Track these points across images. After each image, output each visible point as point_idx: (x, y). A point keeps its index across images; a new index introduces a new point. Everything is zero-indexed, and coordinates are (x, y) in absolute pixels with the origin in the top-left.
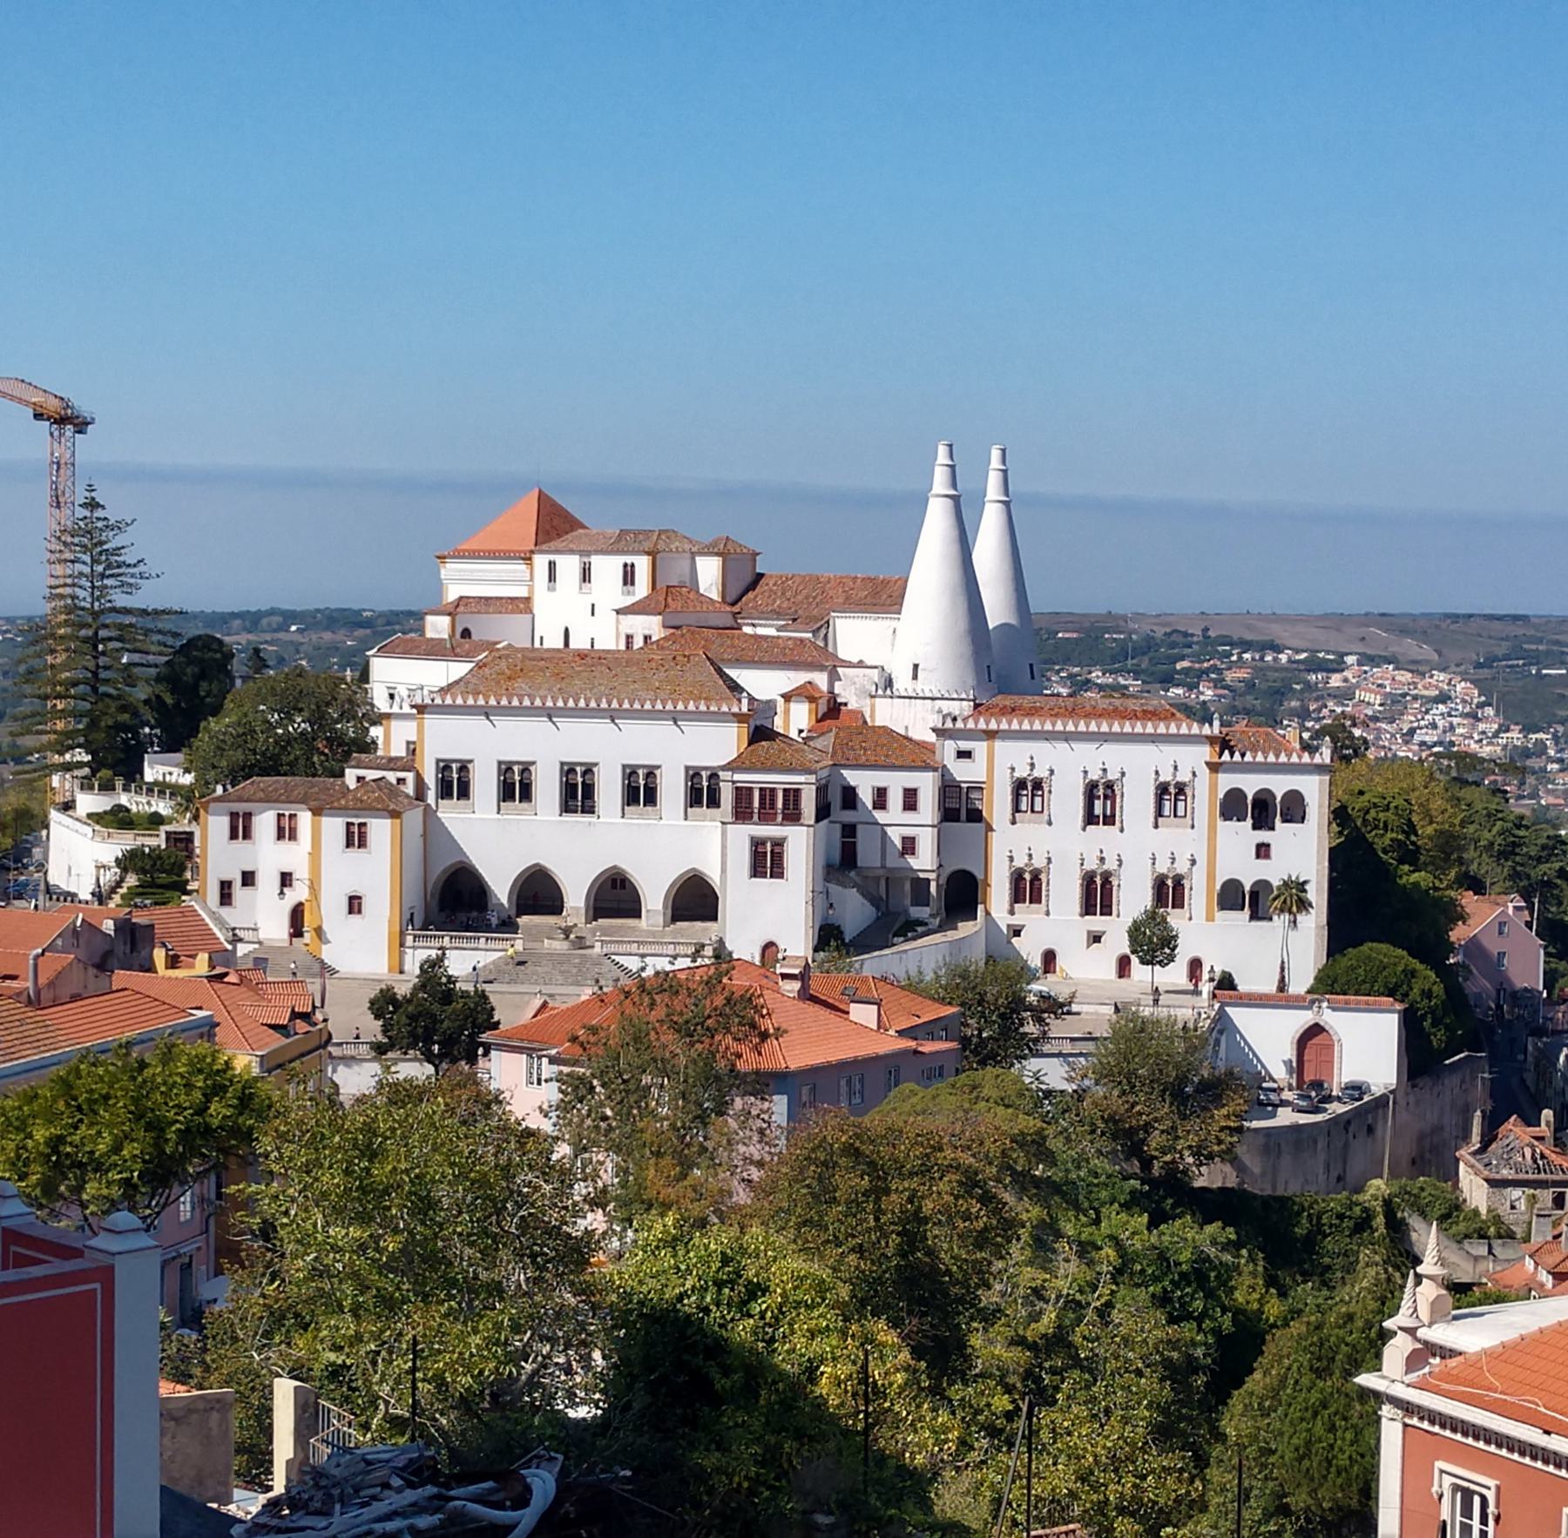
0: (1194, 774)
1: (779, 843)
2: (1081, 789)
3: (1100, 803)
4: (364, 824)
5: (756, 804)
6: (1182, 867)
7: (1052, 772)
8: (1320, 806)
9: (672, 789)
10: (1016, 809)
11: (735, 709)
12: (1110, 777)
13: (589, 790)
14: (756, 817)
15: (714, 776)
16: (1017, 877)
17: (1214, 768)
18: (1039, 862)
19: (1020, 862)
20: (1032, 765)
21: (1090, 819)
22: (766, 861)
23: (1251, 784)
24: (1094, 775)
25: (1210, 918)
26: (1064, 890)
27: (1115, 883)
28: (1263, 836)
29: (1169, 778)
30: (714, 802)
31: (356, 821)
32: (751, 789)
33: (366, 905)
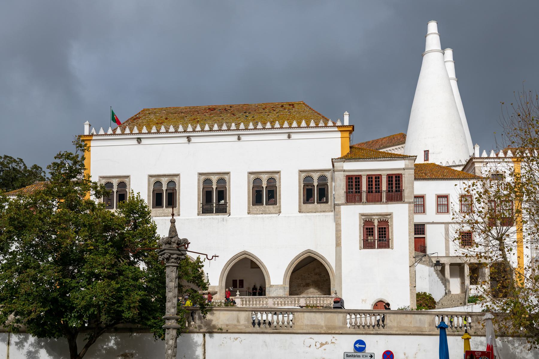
9: (290, 191)
13: (222, 194)
15: (323, 179)
22: (376, 235)
32: (361, 176)
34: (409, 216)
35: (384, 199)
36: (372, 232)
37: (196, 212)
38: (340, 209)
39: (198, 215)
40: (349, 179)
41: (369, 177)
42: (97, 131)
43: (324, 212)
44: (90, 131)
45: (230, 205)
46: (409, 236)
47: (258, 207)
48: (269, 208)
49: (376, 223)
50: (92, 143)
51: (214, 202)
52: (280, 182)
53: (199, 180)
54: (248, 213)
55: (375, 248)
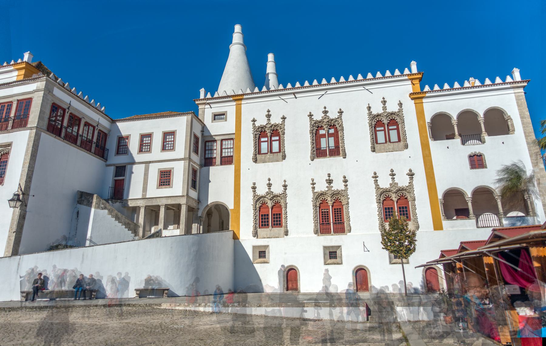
0: (400, 104)
2: (308, 129)
3: (327, 139)
6: (403, 181)
7: (284, 118)
8: (522, 117)
10: (258, 151)
12: (333, 115)
16: (260, 203)
17: (417, 97)
18: (277, 189)
19: (262, 191)
20: (269, 116)
21: (318, 152)
24: (318, 116)
25: (438, 227)
26: (300, 214)
27: (344, 202)
29: (381, 111)
34: (28, 144)
46: (23, 167)
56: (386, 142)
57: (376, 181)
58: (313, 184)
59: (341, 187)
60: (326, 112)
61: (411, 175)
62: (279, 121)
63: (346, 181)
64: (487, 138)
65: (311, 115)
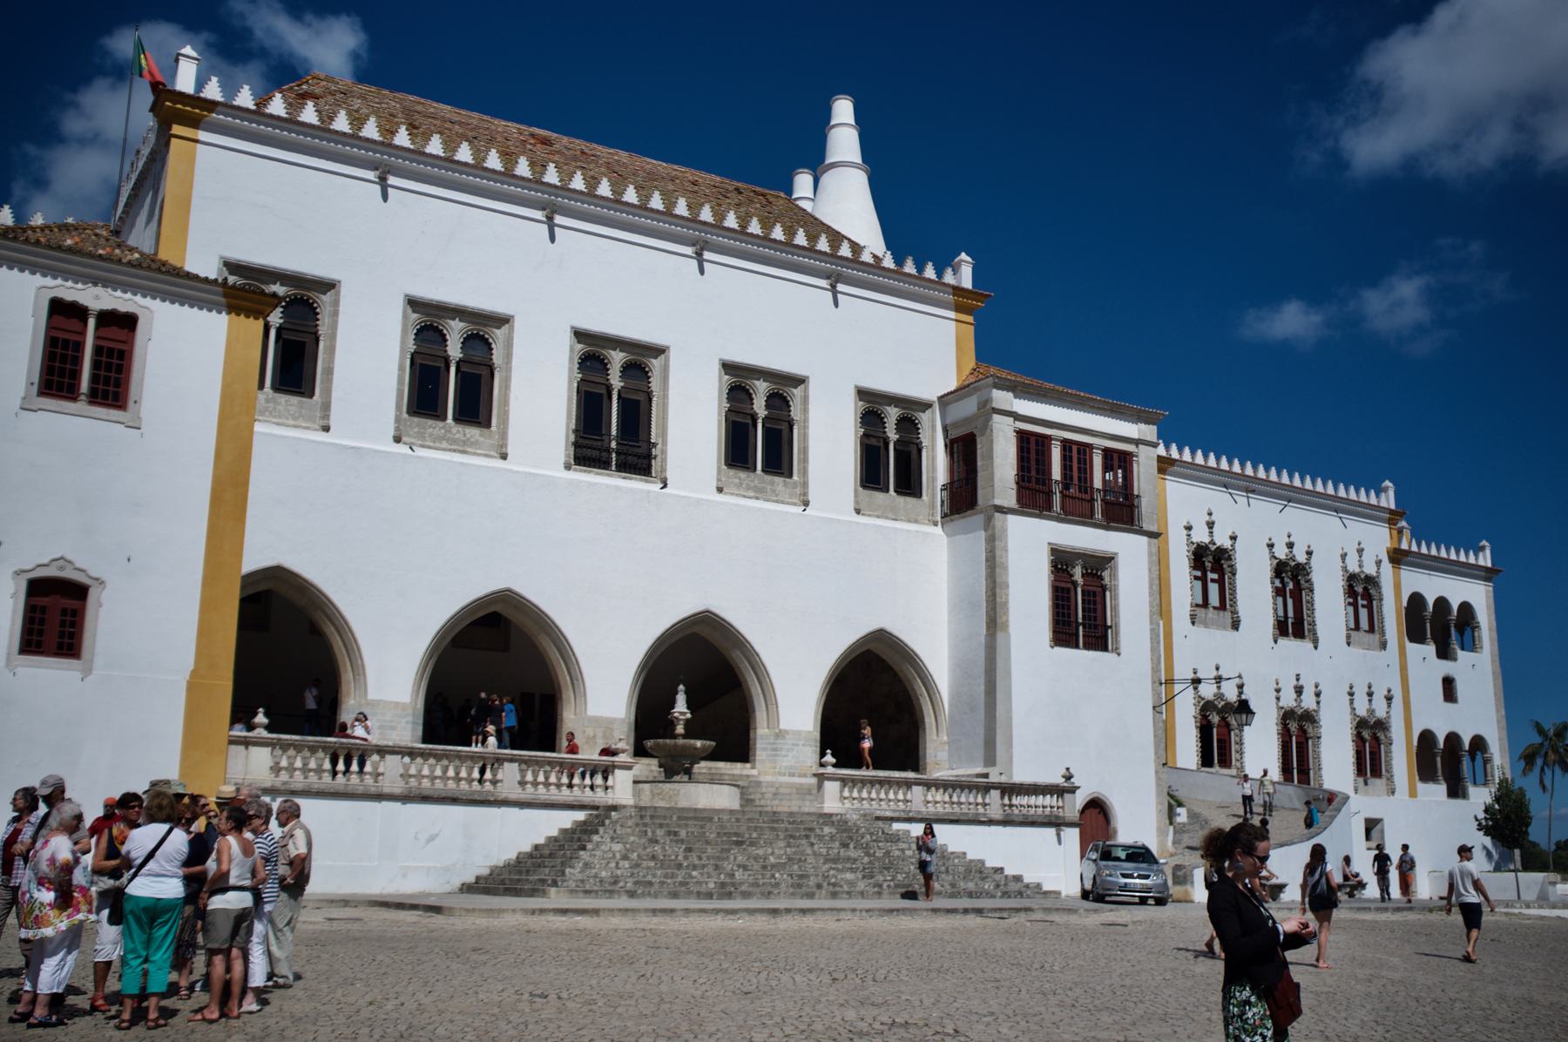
0: (1379, 563)
1: (1098, 565)
4: (128, 322)
5: (1056, 474)
7: (1233, 538)
11: (949, 278)
14: (1057, 499)
20: (1211, 525)
21: (1282, 629)
23: (1433, 586)
24: (1281, 552)
25: (1413, 793)
28: (1446, 667)
30: (909, 484)
31: (98, 298)
32: (1048, 438)
33: (105, 622)
35: (1098, 515)
36: (1069, 600)
37: (562, 459)
38: (1005, 521)
39: (568, 467)
40: (1023, 438)
41: (1067, 445)
42: (230, 88)
43: (916, 521)
44: (201, 83)
45: (664, 452)
47: (742, 475)
48: (772, 483)
49: (1077, 573)
50: (203, 135)
51: (614, 432)
52: (805, 410)
53: (572, 349)
54: (720, 490)
55: (1077, 647)
56: (1357, 627)
57: (1352, 702)
58: (1278, 691)
59: (1313, 706)
60: (1290, 545)
61: (1389, 699)
62: (1227, 544)
63: (1318, 695)
64: (1460, 654)
65: (1271, 546)
